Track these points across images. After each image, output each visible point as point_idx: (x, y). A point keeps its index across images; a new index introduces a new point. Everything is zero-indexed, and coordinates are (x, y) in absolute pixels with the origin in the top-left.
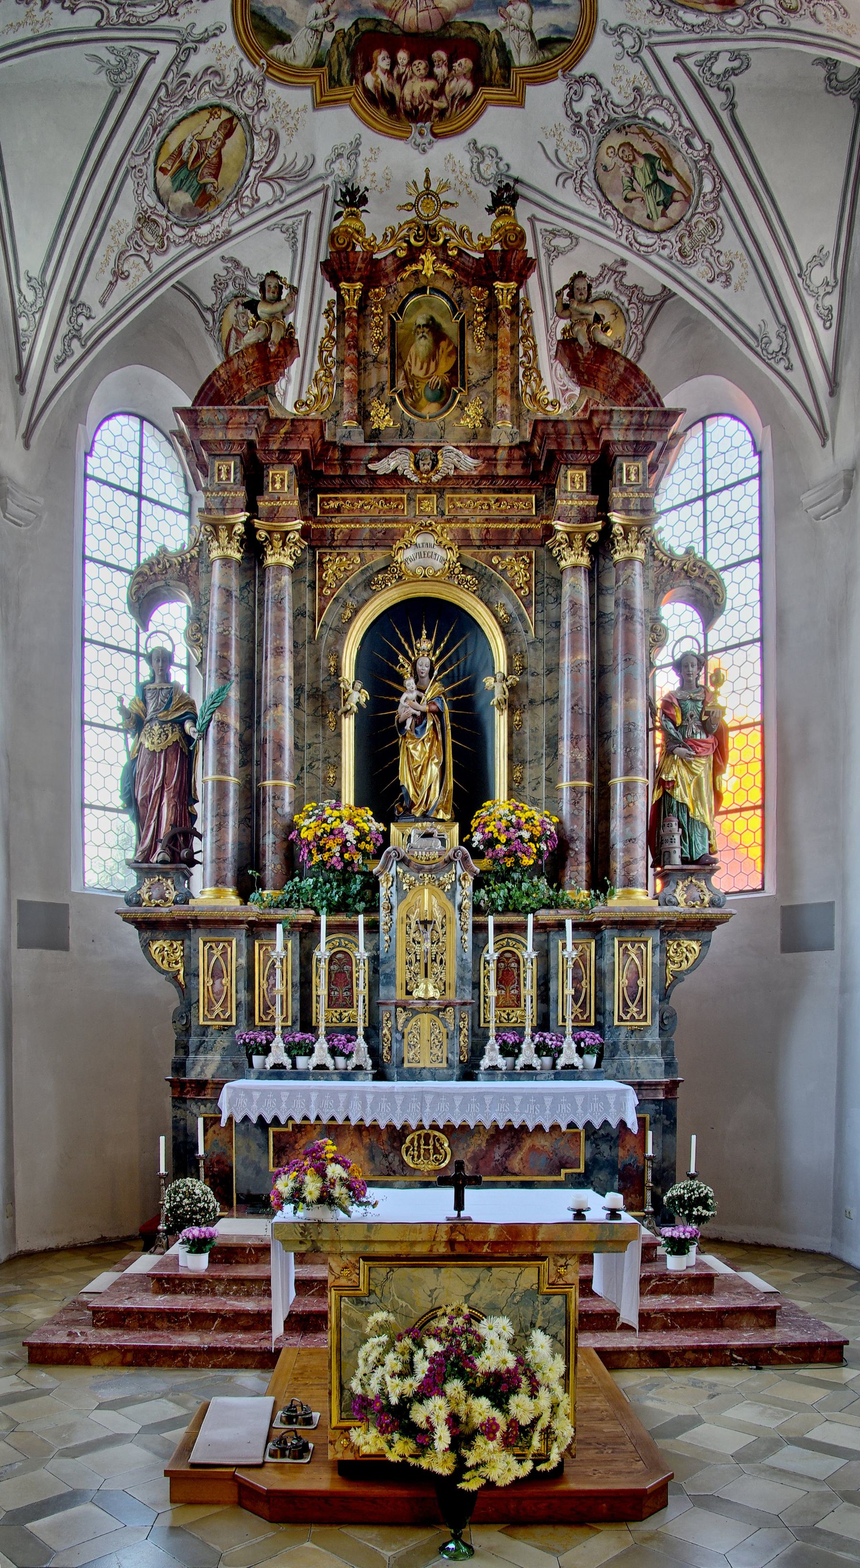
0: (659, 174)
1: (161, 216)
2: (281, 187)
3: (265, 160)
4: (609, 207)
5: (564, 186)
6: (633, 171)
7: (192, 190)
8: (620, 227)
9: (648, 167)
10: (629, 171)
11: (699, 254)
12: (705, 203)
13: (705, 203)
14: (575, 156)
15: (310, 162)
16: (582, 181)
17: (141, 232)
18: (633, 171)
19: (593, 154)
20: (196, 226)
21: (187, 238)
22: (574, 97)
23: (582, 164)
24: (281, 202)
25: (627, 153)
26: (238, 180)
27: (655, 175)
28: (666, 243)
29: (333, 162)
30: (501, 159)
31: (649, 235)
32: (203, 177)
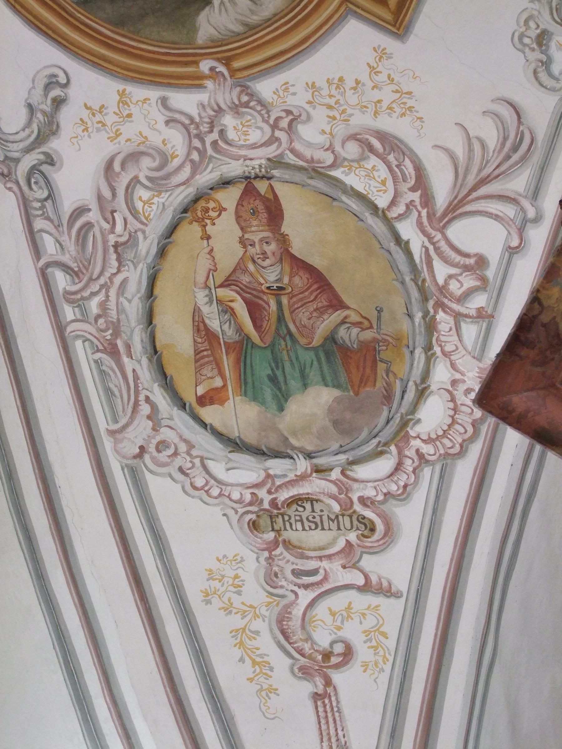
1: (303, 478)
2: (501, 198)
3: (404, 187)
7: (313, 374)
15: (506, 113)
17: (288, 545)
20: (404, 424)
21: (408, 465)
24: (537, 220)
26: (393, 266)
29: (547, 64)
32: (310, 331)
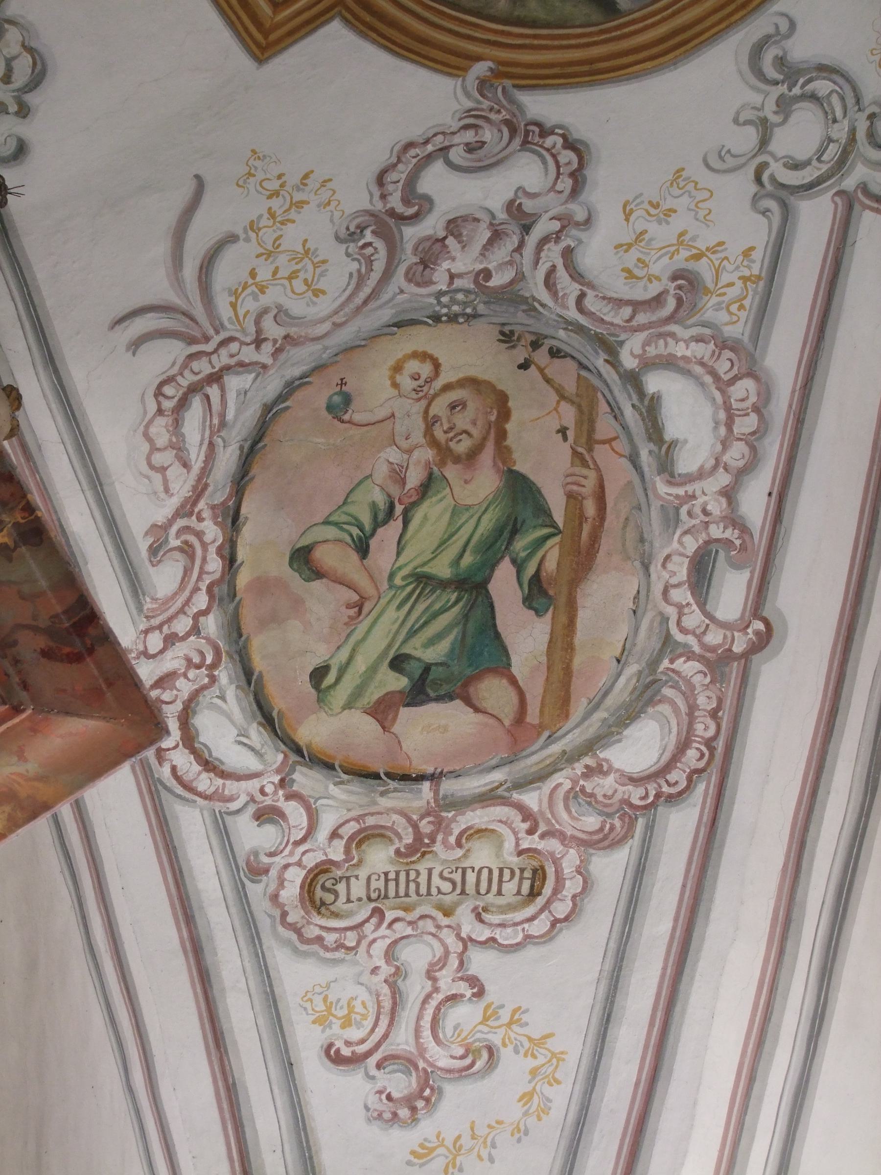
0: (504, 573)
4: (212, 532)
5: (136, 345)
6: (426, 488)
8: (182, 625)
9: (487, 523)
10: (414, 478)
11: (383, 937)
12: (576, 794)
13: (576, 794)
14: (273, 296)
16: (216, 378)
18: (426, 488)
19: (345, 336)
22: (457, 155)
23: (273, 330)
25: (462, 421)
27: (490, 565)
28: (296, 814)
30: (24, 111)
31: (257, 735)
